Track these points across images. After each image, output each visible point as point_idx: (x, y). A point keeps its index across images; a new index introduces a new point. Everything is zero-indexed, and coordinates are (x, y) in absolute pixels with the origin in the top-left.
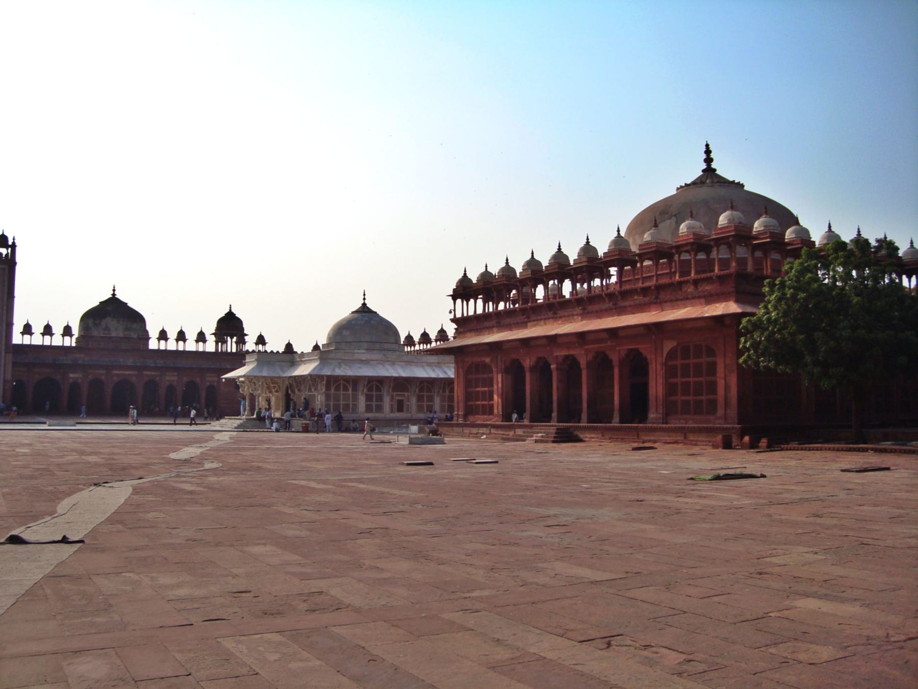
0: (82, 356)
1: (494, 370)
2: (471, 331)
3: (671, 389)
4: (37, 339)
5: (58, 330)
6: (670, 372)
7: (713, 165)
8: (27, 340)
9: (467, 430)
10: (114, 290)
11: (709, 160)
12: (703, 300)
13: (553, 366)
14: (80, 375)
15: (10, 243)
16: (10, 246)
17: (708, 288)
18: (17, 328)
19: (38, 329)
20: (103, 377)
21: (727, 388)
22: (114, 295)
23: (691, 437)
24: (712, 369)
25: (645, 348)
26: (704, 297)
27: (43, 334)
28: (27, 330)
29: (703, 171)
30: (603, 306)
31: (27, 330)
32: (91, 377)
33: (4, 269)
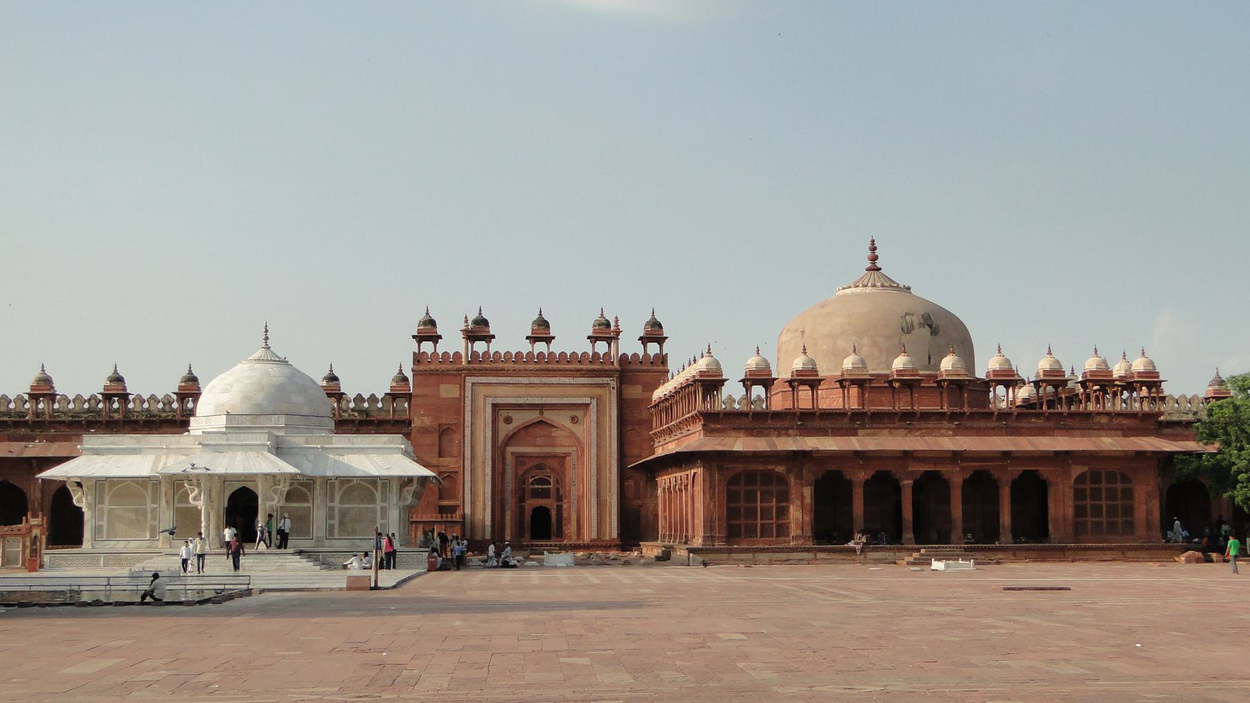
1: (792, 480)
2: (738, 429)
3: (1079, 511)
6: (1079, 494)
7: (879, 264)
9: (734, 556)
11: (874, 259)
12: (1120, 433)
13: (907, 483)
17: (1126, 422)
21: (1149, 512)
23: (1130, 554)
24: (1128, 494)
25: (1045, 471)
26: (1122, 430)
29: (868, 270)
30: (983, 424)
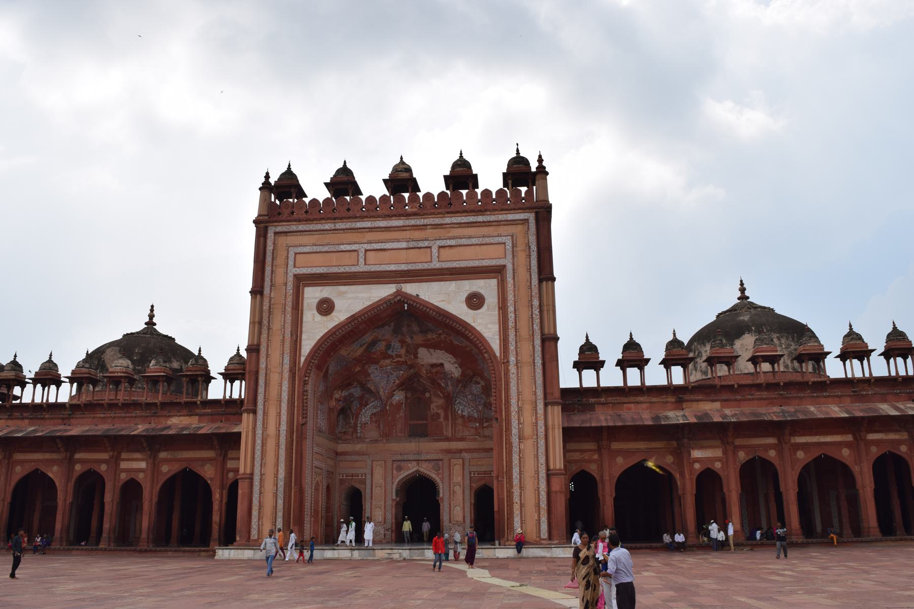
0: (717, 405)
4: (611, 377)
5: (655, 351)
8: (589, 379)
10: (743, 290)
14: (718, 453)
15: (534, 169)
16: (535, 174)
18: (568, 353)
19: (610, 353)
20: (772, 453)
22: (743, 297)
27: (622, 364)
28: (589, 358)
31: (589, 358)
32: (742, 456)
33: (526, 221)
